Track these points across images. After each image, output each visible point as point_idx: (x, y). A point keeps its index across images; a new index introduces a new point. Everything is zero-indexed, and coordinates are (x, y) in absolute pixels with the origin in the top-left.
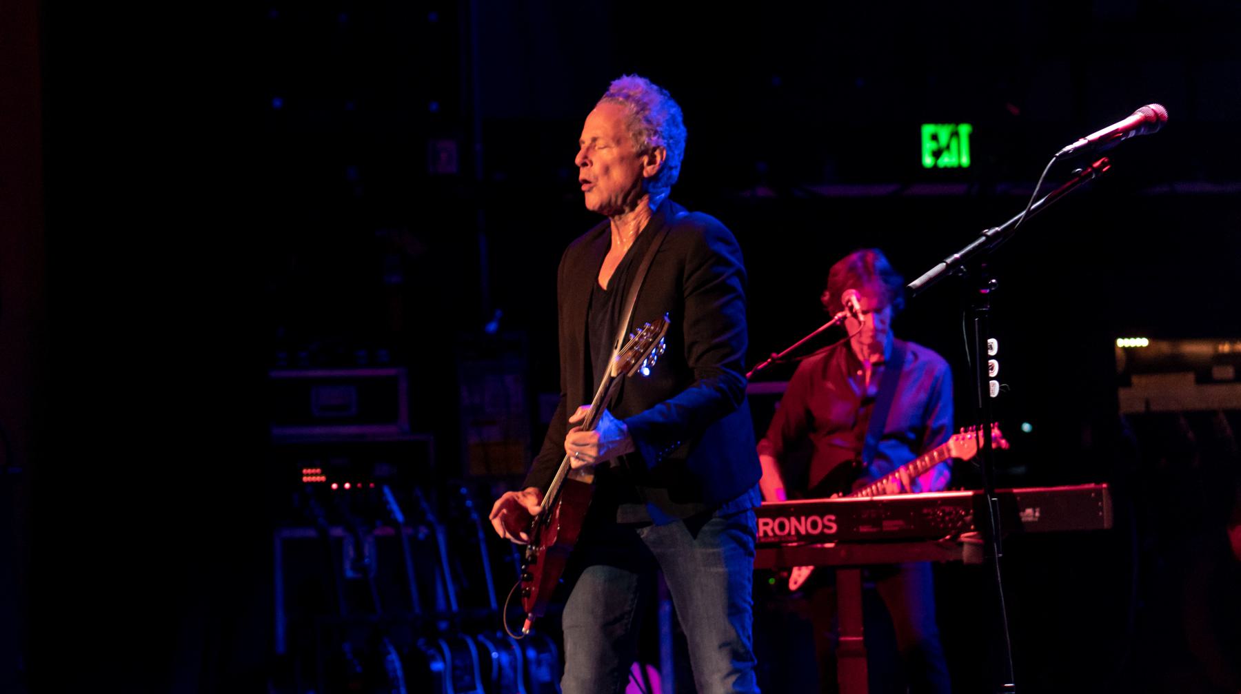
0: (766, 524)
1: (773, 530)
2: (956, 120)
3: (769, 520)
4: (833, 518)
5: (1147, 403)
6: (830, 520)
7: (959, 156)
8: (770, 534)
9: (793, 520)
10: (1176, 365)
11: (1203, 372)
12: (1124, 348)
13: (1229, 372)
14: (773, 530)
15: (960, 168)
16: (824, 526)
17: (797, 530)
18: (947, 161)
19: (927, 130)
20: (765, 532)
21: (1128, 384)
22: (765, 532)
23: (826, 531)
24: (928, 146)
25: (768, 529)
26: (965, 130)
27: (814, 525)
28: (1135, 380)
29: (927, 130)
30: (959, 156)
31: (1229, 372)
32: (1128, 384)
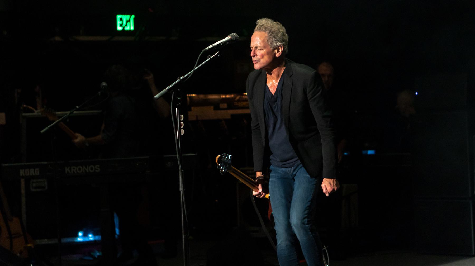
0: (74, 169)
1: (76, 171)
2: (131, 14)
3: (74, 167)
4: (99, 166)
5: (197, 116)
6: (98, 167)
7: (131, 27)
8: (75, 172)
9: (84, 167)
10: (207, 103)
11: (216, 105)
12: (189, 97)
13: (225, 106)
14: (76, 171)
15: (130, 30)
16: (95, 169)
17: (85, 171)
18: (127, 28)
19: (119, 17)
20: (74, 171)
21: (190, 110)
22: (74, 171)
23: (96, 171)
24: (119, 22)
25: (75, 170)
26: (133, 16)
27: (92, 169)
28: (192, 108)
29: (119, 17)
30: (131, 27)
31: (225, 106)
32: (190, 110)
